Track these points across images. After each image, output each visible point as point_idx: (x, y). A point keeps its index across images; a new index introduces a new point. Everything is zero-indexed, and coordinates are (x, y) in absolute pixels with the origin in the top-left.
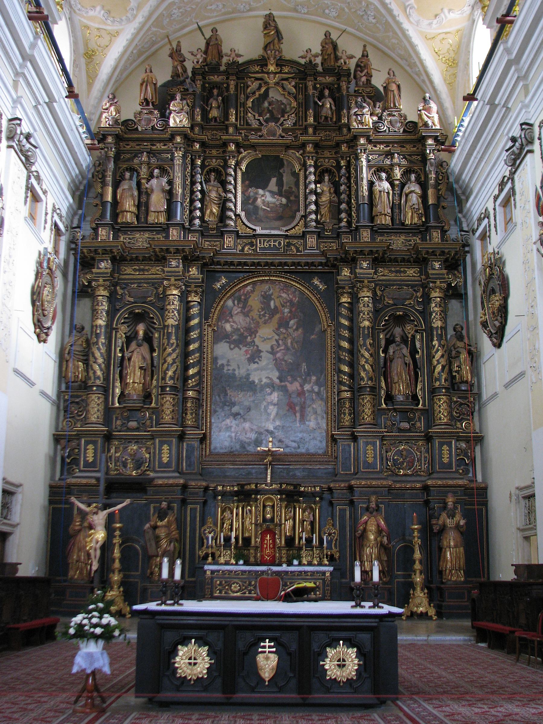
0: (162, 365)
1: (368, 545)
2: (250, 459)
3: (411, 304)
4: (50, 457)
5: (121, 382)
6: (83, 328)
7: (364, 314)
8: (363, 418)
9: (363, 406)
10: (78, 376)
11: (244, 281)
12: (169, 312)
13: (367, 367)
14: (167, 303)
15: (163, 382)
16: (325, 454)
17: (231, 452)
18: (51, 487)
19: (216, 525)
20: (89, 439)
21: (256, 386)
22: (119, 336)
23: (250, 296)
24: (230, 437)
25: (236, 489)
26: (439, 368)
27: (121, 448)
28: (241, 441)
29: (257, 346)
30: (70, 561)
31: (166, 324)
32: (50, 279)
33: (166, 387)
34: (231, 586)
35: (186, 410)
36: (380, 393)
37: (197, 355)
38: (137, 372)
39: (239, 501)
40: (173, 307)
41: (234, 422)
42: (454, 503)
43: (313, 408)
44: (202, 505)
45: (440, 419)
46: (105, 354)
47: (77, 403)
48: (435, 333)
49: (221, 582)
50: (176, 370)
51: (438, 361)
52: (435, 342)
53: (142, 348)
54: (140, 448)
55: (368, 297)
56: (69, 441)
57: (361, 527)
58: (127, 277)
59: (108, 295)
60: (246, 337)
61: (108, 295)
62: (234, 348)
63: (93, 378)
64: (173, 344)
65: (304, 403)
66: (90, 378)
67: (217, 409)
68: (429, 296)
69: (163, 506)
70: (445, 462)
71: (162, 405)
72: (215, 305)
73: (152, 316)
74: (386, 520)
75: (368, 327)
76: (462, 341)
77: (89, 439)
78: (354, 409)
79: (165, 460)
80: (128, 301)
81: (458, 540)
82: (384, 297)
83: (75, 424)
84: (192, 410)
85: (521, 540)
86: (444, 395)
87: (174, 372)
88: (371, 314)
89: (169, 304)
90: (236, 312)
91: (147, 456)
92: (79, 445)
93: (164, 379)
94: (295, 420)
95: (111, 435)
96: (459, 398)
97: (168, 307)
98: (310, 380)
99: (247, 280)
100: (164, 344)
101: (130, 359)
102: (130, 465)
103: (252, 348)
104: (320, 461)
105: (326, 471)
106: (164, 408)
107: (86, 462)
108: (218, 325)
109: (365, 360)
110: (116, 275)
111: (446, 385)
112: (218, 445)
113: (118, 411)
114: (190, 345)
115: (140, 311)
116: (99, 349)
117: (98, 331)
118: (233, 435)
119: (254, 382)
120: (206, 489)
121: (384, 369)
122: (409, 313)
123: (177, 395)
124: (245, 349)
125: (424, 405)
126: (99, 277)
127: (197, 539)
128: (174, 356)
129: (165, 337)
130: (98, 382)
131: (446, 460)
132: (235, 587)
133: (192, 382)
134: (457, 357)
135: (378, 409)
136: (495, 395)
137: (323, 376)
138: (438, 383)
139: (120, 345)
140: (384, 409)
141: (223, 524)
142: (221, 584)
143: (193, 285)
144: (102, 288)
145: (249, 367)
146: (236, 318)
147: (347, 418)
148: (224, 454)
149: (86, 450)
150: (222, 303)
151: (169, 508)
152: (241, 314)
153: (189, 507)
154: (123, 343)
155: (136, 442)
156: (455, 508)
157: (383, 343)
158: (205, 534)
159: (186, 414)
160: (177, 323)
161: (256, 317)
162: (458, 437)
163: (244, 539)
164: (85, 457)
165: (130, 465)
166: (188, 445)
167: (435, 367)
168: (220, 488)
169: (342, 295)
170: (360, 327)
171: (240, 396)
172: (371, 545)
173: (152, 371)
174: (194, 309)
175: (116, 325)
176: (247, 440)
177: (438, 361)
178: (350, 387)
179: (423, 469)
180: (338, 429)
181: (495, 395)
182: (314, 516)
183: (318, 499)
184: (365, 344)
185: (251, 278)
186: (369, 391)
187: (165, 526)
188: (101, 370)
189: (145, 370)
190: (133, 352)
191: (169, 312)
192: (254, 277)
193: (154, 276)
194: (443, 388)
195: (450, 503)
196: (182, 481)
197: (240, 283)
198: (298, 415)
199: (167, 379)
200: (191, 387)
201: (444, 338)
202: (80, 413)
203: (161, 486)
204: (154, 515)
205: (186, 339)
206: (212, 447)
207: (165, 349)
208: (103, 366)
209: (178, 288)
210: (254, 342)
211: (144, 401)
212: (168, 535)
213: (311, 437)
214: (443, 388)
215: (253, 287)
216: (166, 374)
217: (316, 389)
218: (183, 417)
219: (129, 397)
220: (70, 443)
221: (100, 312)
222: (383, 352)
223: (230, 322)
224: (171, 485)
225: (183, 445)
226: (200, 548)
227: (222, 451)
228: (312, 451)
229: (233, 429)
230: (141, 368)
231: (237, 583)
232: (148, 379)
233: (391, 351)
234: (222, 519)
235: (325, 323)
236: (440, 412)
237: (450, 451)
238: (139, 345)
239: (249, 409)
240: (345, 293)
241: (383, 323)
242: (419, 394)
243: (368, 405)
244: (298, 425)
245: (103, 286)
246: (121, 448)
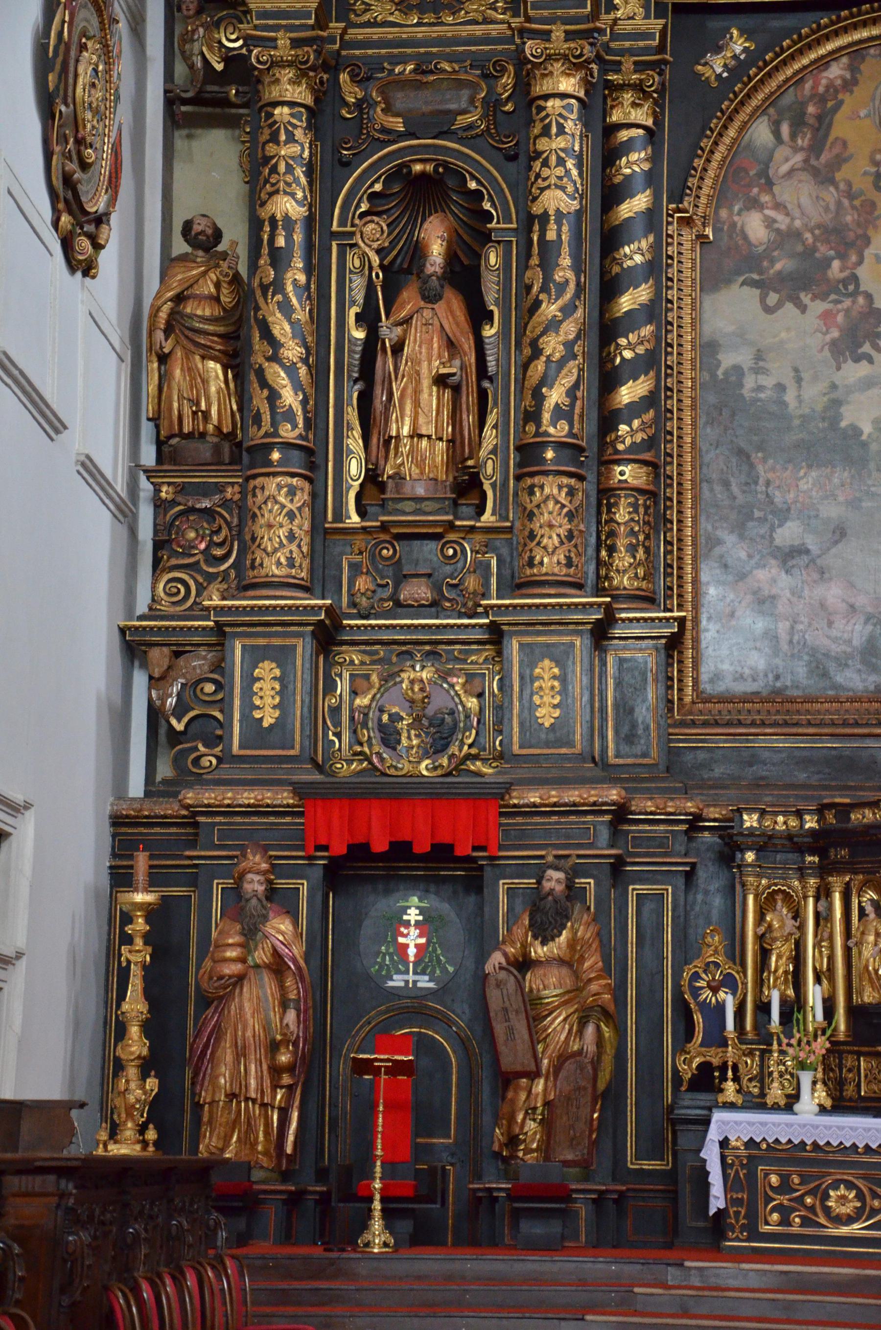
0: (526, 366)
2: (851, 718)
4: (111, 709)
5: (366, 438)
6: (218, 235)
10: (206, 415)
11: (818, 42)
12: (545, 164)
14: (536, 131)
15: (531, 428)
17: (777, 692)
18: (118, 821)
19: (736, 954)
20: (262, 642)
21: (864, 445)
22: (353, 261)
23: (841, 103)
24: (771, 637)
25: (811, 823)
27: (374, 678)
28: (814, 652)
29: (869, 297)
30: (205, 1096)
31: (537, 209)
32: (95, 21)
33: (544, 445)
34: (826, 1197)
35: (612, 534)
37: (647, 330)
38: (425, 396)
39: (824, 870)
40: (560, 143)
41: (784, 580)
44: (681, 881)
46: (307, 329)
47: (209, 513)
49: (785, 1179)
50: (576, 385)
53: (440, 307)
54: (444, 675)
56: (177, 654)
58: (376, 33)
59: (309, 100)
60: (826, 263)
61: (309, 100)
62: (779, 305)
63: (266, 418)
64: (562, 287)
66: (257, 419)
67: (719, 533)
69: (547, 885)
71: (531, 516)
72: (707, 144)
73: (473, 185)
77: (262, 642)
79: (546, 715)
80: (384, 130)
83: (200, 589)
84: (633, 533)
87: (571, 393)
89: (546, 132)
90: (785, 168)
91: (472, 703)
92: (220, 666)
93: (532, 416)
95: (339, 627)
97: (543, 144)
99: (827, 38)
100: (529, 288)
101: (398, 349)
102: (410, 740)
103: (847, 303)
106: (536, 526)
107: (252, 725)
108: (717, 219)
110: (336, 27)
112: (726, 667)
113: (359, 541)
114: (622, 293)
115: (429, 168)
116: (286, 308)
117: (281, 242)
118: (783, 627)
119: (857, 432)
120: (695, 823)
123: (581, 478)
124: (818, 307)
126: (276, 28)
127: (668, 1012)
128: (569, 329)
129: (535, 261)
130: (288, 433)
132: (843, 1199)
133: (633, 433)
139: (360, 298)
141: (764, 954)
142: (785, 1187)
143: (628, 64)
144: (288, 74)
145: (838, 378)
146: (784, 192)
148: (746, 698)
149: (250, 680)
150: (732, 133)
151: (573, 893)
152: (804, 176)
153: (634, 889)
154: (370, 288)
155: (428, 654)
158: (695, 992)
159: (612, 550)
160: (575, 205)
161: (863, 184)
163: (853, 1011)
164: (249, 706)
165: (410, 740)
166: (622, 661)
168: (750, 821)
171: (803, 486)
173: (483, 395)
174: (634, 156)
175: (342, 223)
176: (836, 649)
185: (845, 30)
187: (561, 961)
188: (297, 386)
189: (456, 389)
190: (407, 321)
191: (545, 164)
192: (855, 27)
193: (478, 30)
196: (614, 794)
197: (801, 52)
199: (546, 416)
200: (628, 450)
202: (219, 552)
203: (534, 811)
204: (512, 917)
205: (603, 272)
206: (706, 670)
207: (537, 304)
208: (303, 371)
209: (577, 67)
210: (855, 279)
211: (455, 503)
212: (575, 992)
215: (853, 69)
216: (539, 398)
218: (599, 563)
219: (398, 488)
220: (181, 661)
221: (282, 168)
223: (760, 207)
224: (573, 809)
225: (604, 663)
226: (680, 1046)
227: (749, 687)
229: (782, 607)
230: (441, 381)
231: (850, 1186)
232: (469, 419)
234: (760, 938)
238: (431, 297)
239: (840, 533)
245: (290, 64)
246: (374, 678)
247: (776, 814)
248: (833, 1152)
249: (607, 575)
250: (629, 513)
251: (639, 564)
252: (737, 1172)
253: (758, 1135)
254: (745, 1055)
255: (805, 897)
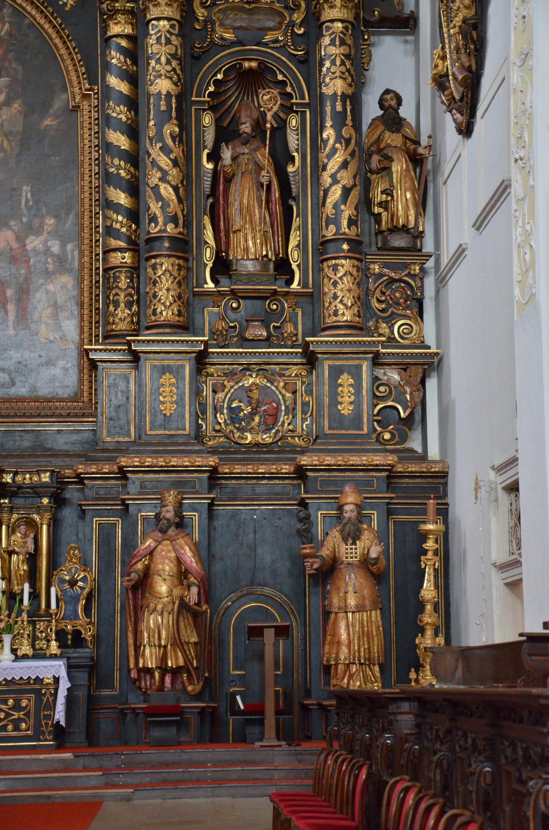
1: (152, 605)
3: (276, 41)
7: (158, 61)
8: (154, 313)
9: (155, 283)
13: (167, 191)
16: (75, 398)
26: (336, 193)
36: (200, 254)
42: (359, 507)
43: (47, 292)
45: (336, 313)
48: (328, 109)
51: (333, 176)
52: (329, 133)
55: (169, 19)
57: (140, 566)
65: (27, 279)
68: (319, 19)
70: (345, 412)
74: (196, 548)
75: (169, 95)
76: (398, 131)
78: (138, 293)
81: (366, 592)
82: (213, 23)
85: (505, 590)
86: (345, 258)
88: (174, 63)
94: (5, 320)
96: (386, 265)
98: (41, 226)
104: (61, 416)
105: (75, 437)
109: (159, 175)
111: (352, 232)
121: (211, 200)
122: (272, 64)
125: (304, 283)
131: (346, 409)
134: (386, 170)
135: (196, 294)
136: (461, 252)
137: (71, 217)
138: (332, 228)
140: (209, 294)
147: (122, 312)
156: (361, 518)
157: (210, 137)
162: (377, 355)
167: (326, 192)
169: (111, 17)
170: (149, 95)
172: (159, 607)
177: (333, 176)
178: (130, 241)
179: (299, 430)
180: (105, 337)
181: (461, 252)
182: (37, 541)
183: (45, 501)
184: (160, 137)
186: (169, 249)
194: (344, 240)
195: (347, 508)
198: (11, 307)
201: (349, 122)
213: (43, 360)
214: (344, 240)
217: (55, 248)
222: (210, 158)
228: (44, 391)
233: (227, 154)
235: (77, 90)
236: (335, 297)
237: (358, 387)
240: (117, 11)
241: (211, 89)
242: (294, 257)
243: (166, 282)
244: (12, 332)
247: (24, 473)
248: (24, 684)
249: (114, 321)
250: (128, 283)
251: (133, 314)
252: (48, 699)
253: (33, 675)
254: (88, 625)
255: (42, 524)
